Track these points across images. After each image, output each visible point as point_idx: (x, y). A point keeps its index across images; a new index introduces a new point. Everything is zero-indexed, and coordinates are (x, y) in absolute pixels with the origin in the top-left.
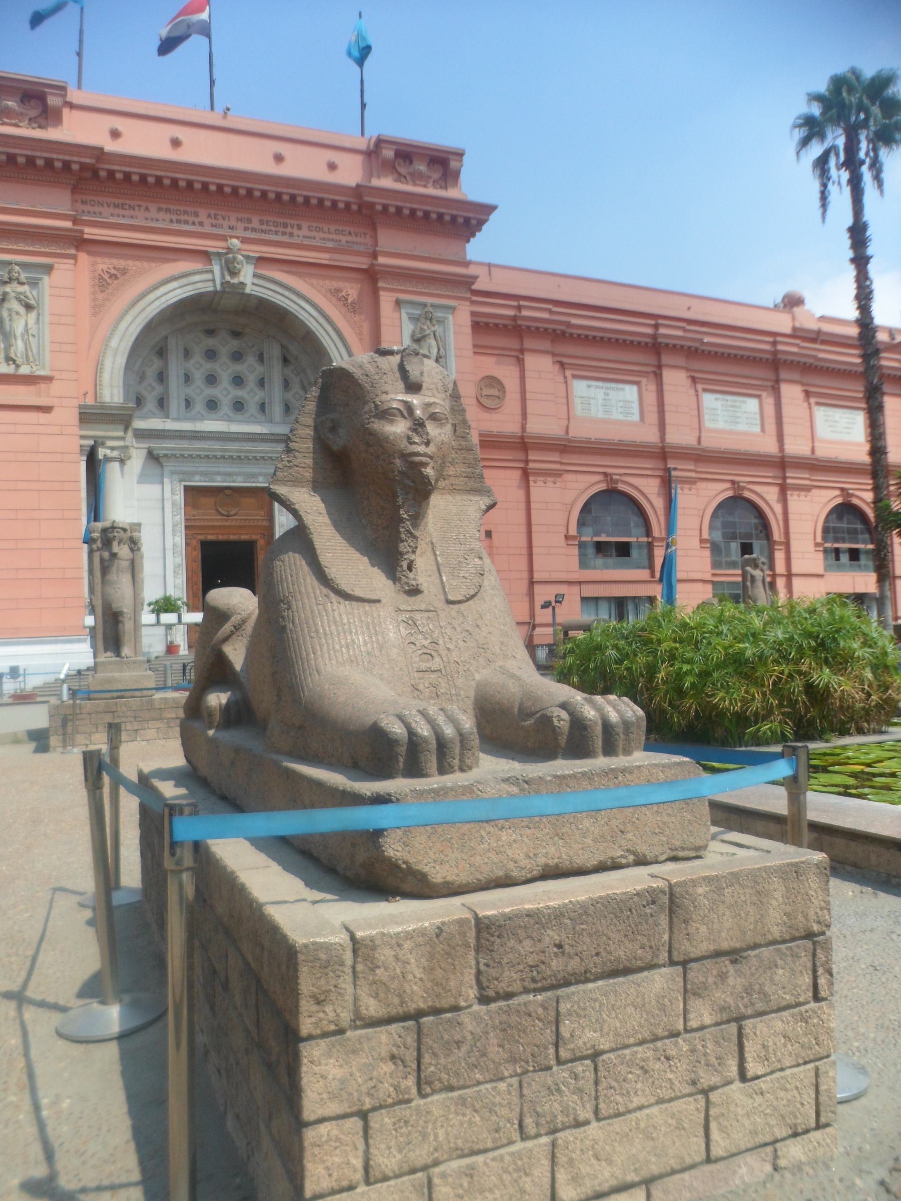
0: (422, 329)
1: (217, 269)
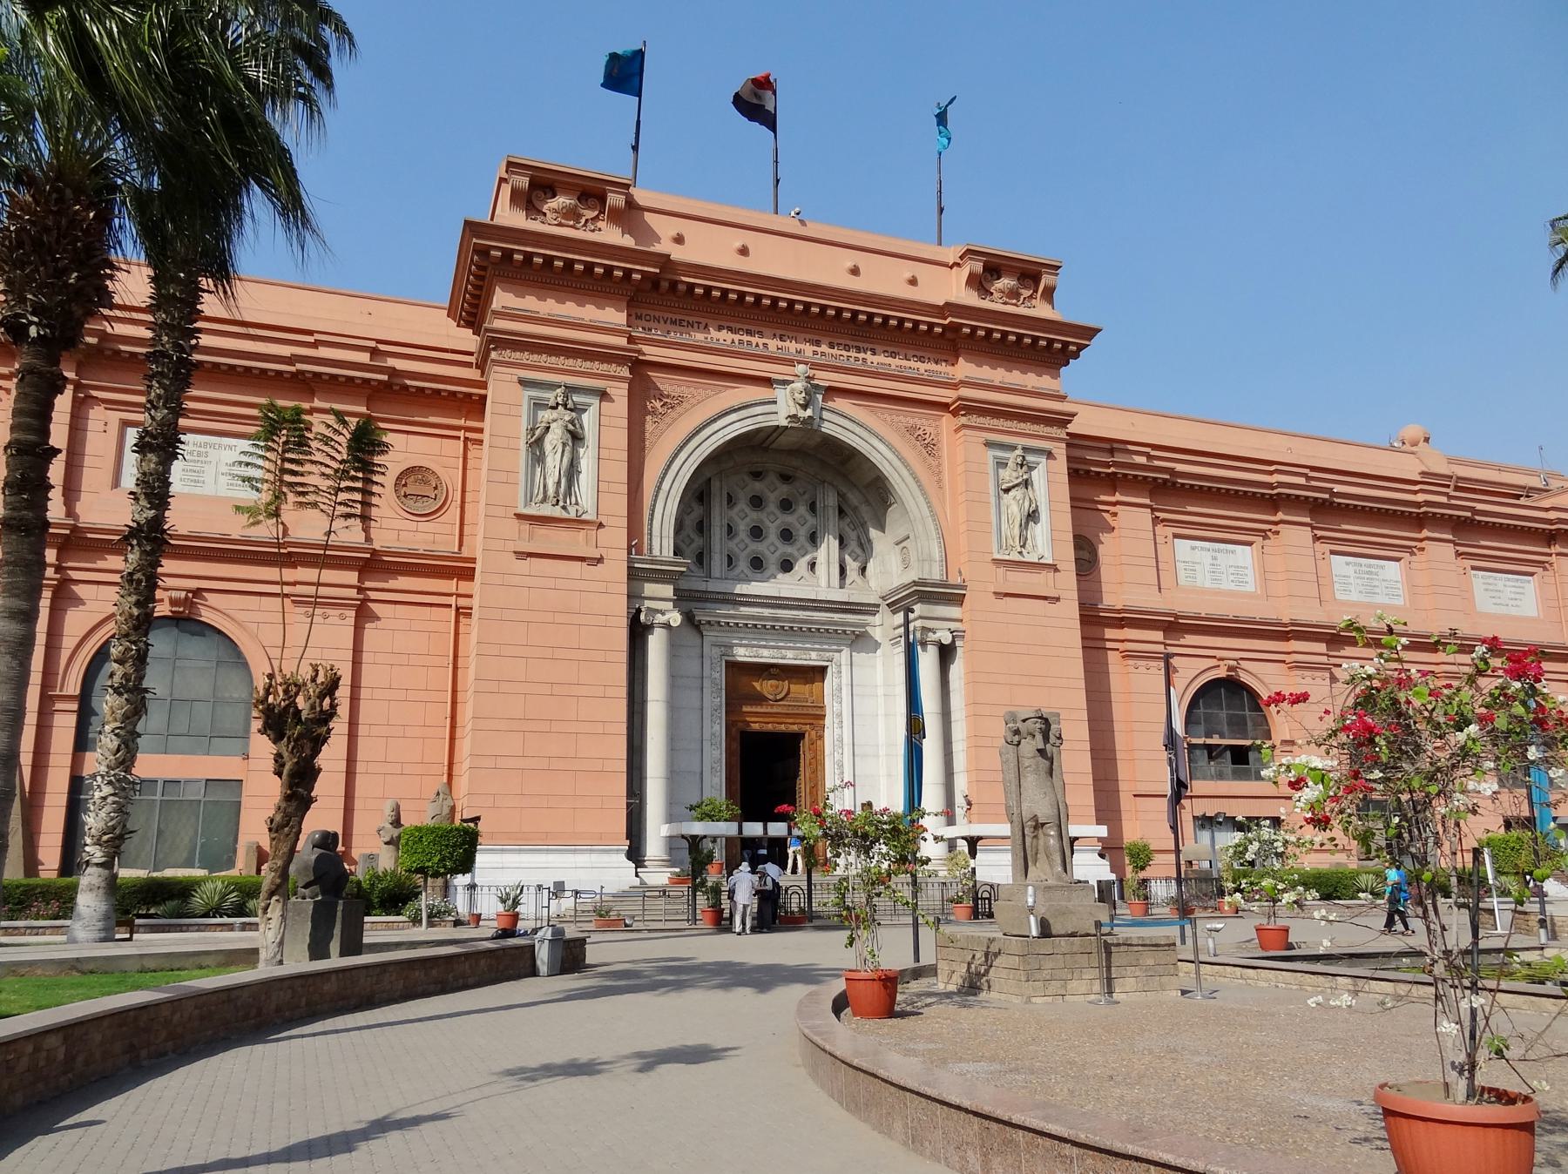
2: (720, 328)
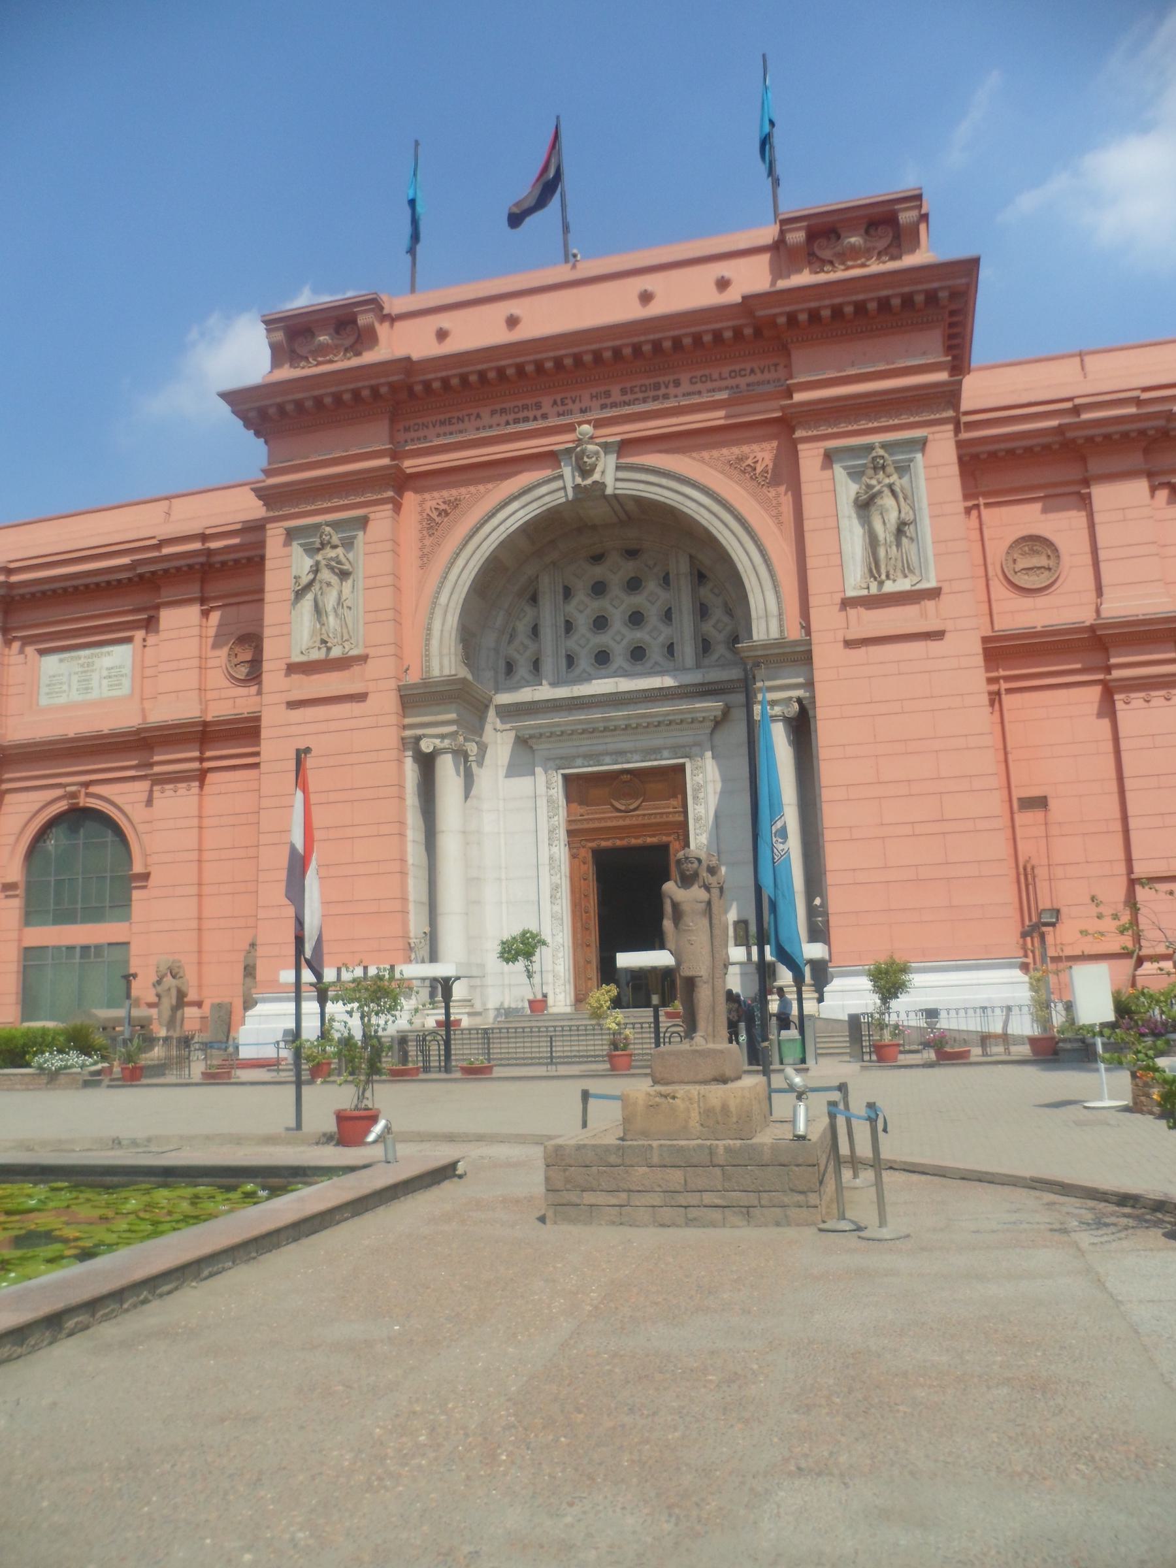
1: (567, 471)
2: (493, 413)
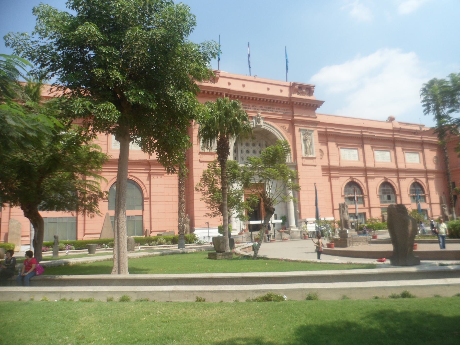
0: (306, 137)
1: (254, 121)
